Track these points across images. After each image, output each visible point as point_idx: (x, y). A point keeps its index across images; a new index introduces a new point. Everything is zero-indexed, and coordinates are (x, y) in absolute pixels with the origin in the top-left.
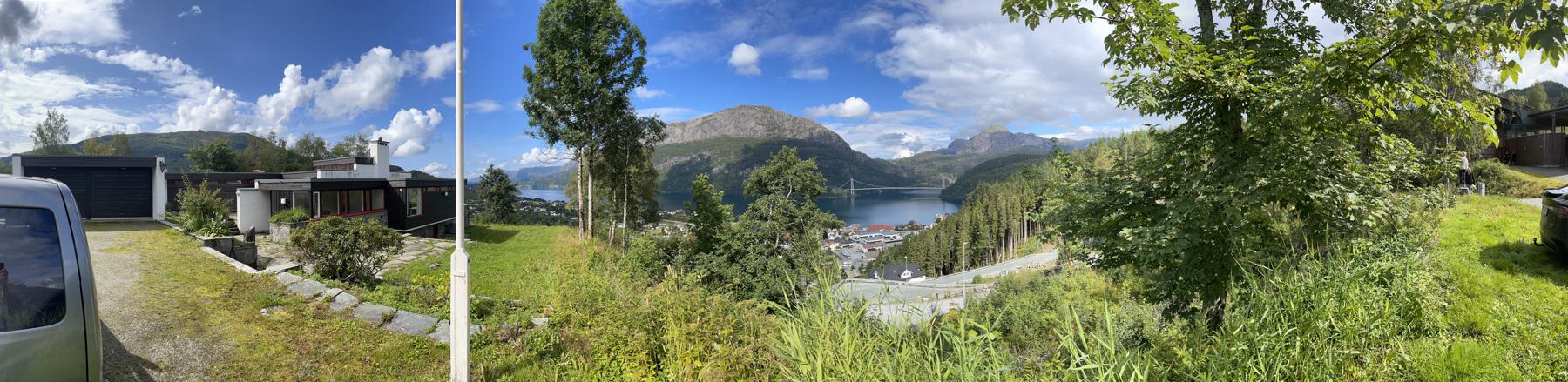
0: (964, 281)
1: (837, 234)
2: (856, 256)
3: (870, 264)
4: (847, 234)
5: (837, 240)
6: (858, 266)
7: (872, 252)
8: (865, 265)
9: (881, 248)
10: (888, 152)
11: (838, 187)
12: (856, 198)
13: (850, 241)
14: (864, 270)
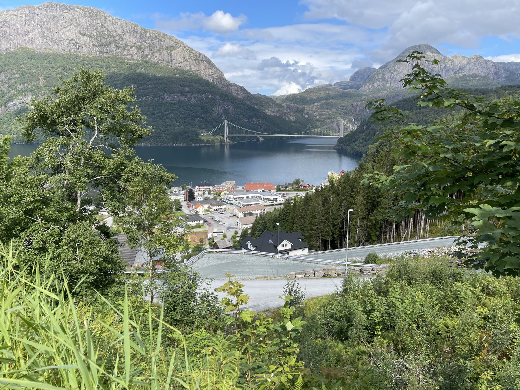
0: (358, 259)
1: (207, 193)
2: (229, 222)
3: (245, 232)
4: (219, 195)
5: (206, 201)
6: (230, 234)
7: (248, 217)
8: (240, 233)
9: (259, 212)
10: (271, 85)
11: (209, 130)
12: (231, 147)
13: (222, 203)
14: (238, 239)
